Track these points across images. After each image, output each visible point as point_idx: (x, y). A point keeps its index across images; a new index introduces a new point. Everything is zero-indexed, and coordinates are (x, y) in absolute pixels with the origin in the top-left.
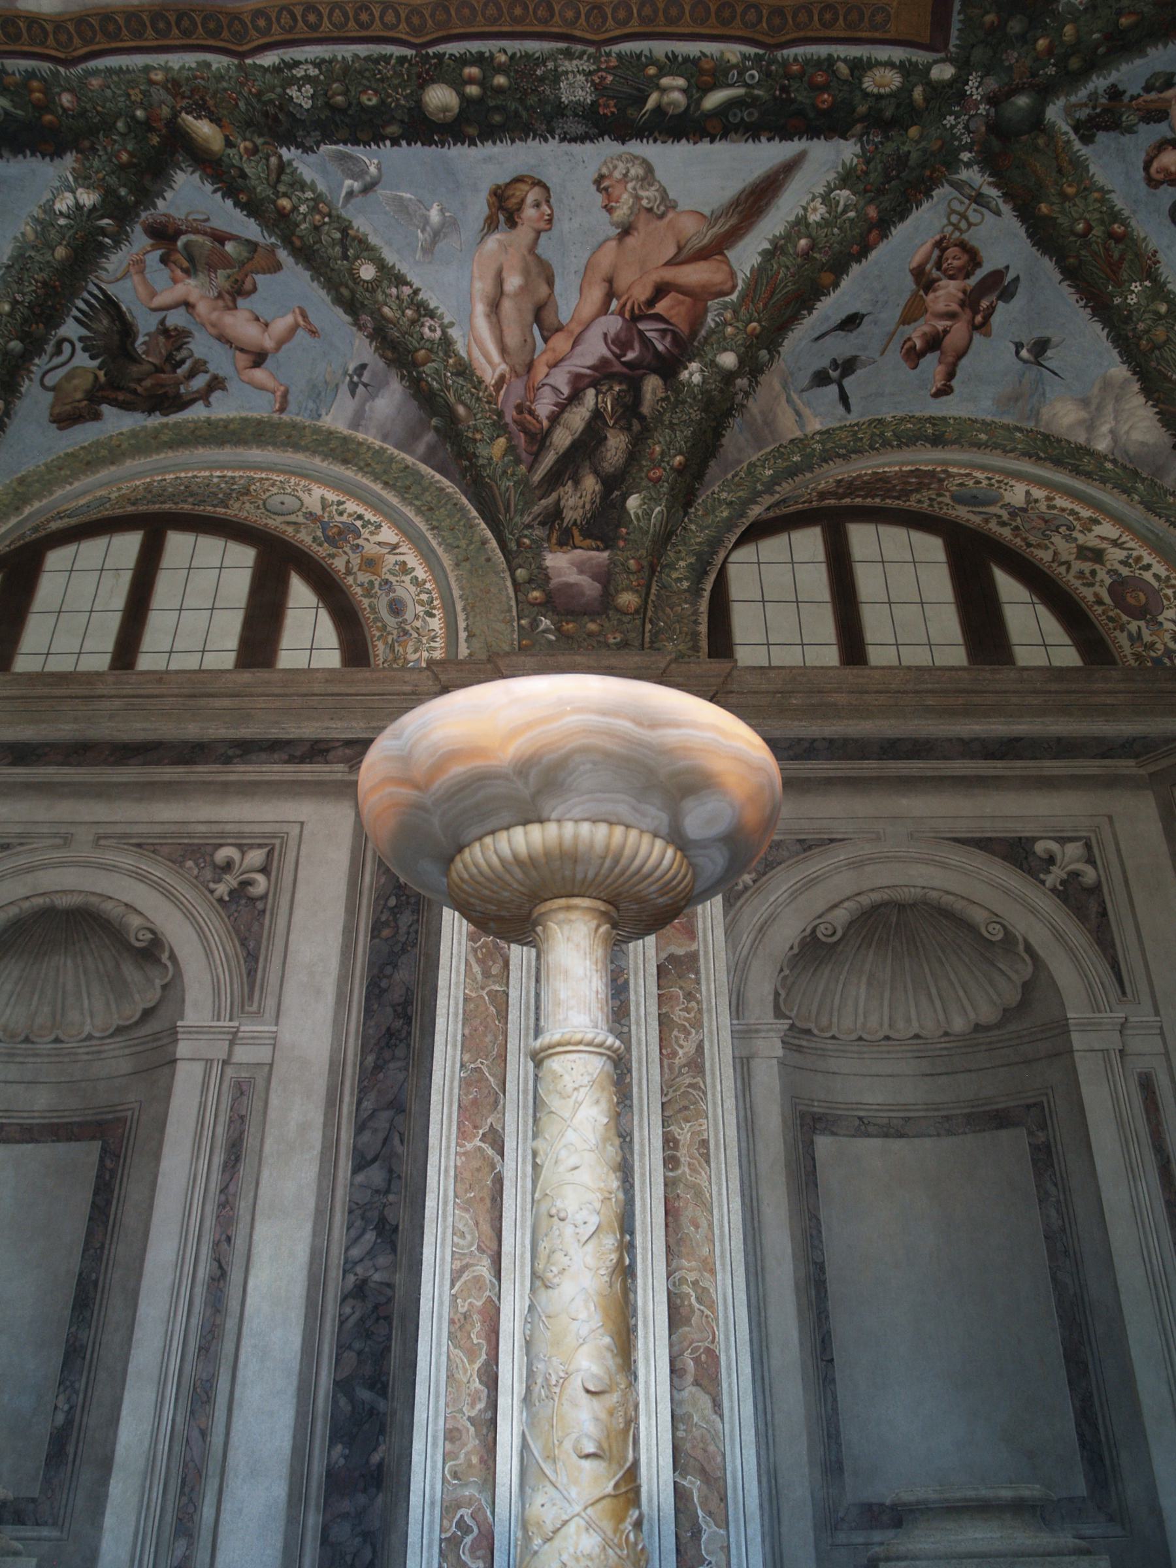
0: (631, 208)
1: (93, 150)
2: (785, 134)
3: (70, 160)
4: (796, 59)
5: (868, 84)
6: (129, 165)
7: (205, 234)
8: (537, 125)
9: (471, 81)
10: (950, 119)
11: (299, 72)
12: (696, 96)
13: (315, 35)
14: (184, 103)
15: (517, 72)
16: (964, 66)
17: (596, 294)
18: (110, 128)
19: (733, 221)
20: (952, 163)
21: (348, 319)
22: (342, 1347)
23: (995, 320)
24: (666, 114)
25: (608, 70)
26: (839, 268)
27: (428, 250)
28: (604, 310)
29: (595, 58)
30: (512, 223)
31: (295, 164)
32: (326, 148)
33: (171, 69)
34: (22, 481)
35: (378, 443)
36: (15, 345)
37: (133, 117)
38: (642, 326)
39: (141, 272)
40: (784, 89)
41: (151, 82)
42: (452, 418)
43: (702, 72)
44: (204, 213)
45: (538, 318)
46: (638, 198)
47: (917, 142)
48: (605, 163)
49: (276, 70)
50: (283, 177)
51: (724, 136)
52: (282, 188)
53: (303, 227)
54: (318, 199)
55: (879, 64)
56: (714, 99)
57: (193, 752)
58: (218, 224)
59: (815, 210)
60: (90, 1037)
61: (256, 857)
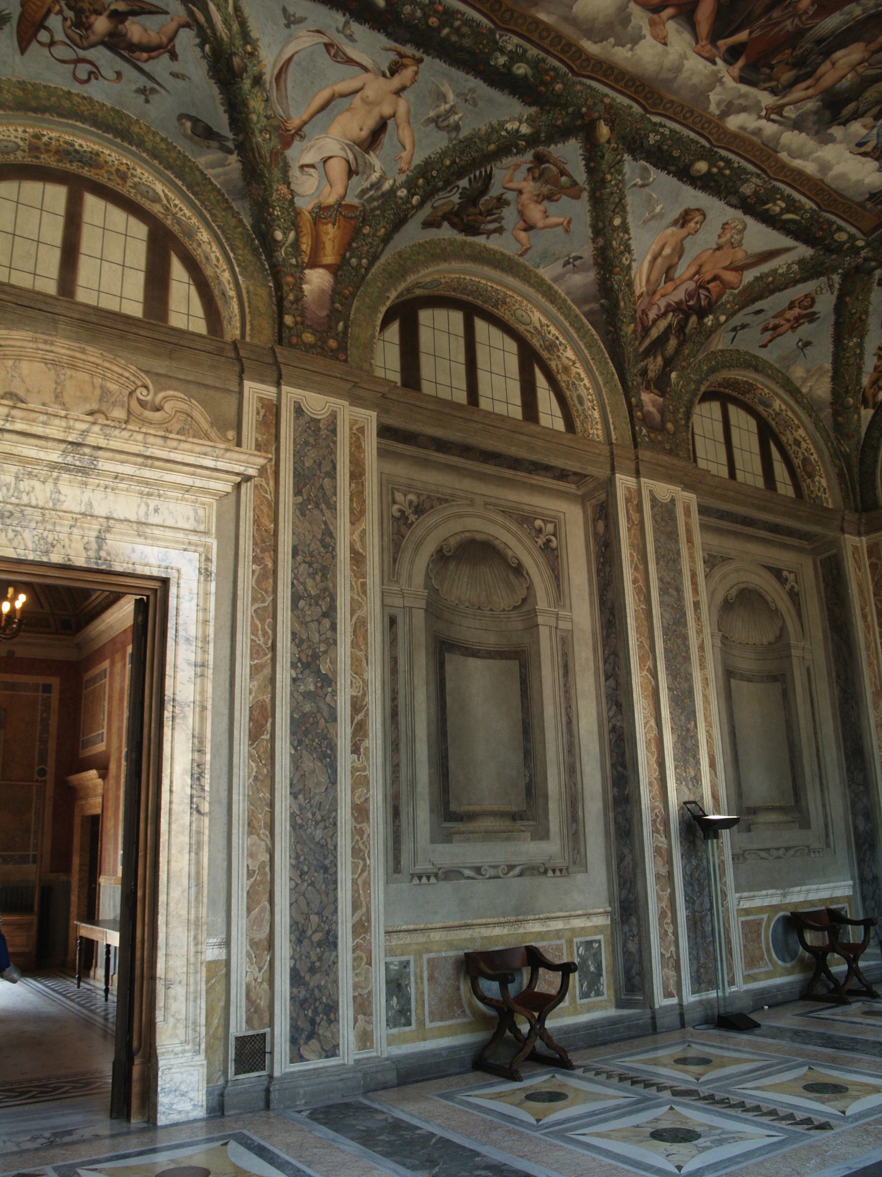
1: (549, 112)
2: (797, 238)
3: (533, 110)
5: (836, 236)
7: (558, 168)
11: (661, 130)
14: (607, 116)
16: (868, 245)
17: (693, 270)
18: (565, 107)
20: (834, 270)
21: (591, 236)
22: (611, 751)
23: (801, 328)
26: (772, 292)
27: (645, 222)
28: (691, 279)
29: (765, 182)
30: (683, 226)
34: (400, 255)
35: (563, 295)
36: (440, 184)
37: (580, 110)
38: (701, 291)
39: (515, 170)
41: (602, 101)
42: (616, 305)
45: (667, 272)
49: (655, 124)
57: (515, 463)
58: (569, 168)
60: (504, 610)
61: (550, 528)
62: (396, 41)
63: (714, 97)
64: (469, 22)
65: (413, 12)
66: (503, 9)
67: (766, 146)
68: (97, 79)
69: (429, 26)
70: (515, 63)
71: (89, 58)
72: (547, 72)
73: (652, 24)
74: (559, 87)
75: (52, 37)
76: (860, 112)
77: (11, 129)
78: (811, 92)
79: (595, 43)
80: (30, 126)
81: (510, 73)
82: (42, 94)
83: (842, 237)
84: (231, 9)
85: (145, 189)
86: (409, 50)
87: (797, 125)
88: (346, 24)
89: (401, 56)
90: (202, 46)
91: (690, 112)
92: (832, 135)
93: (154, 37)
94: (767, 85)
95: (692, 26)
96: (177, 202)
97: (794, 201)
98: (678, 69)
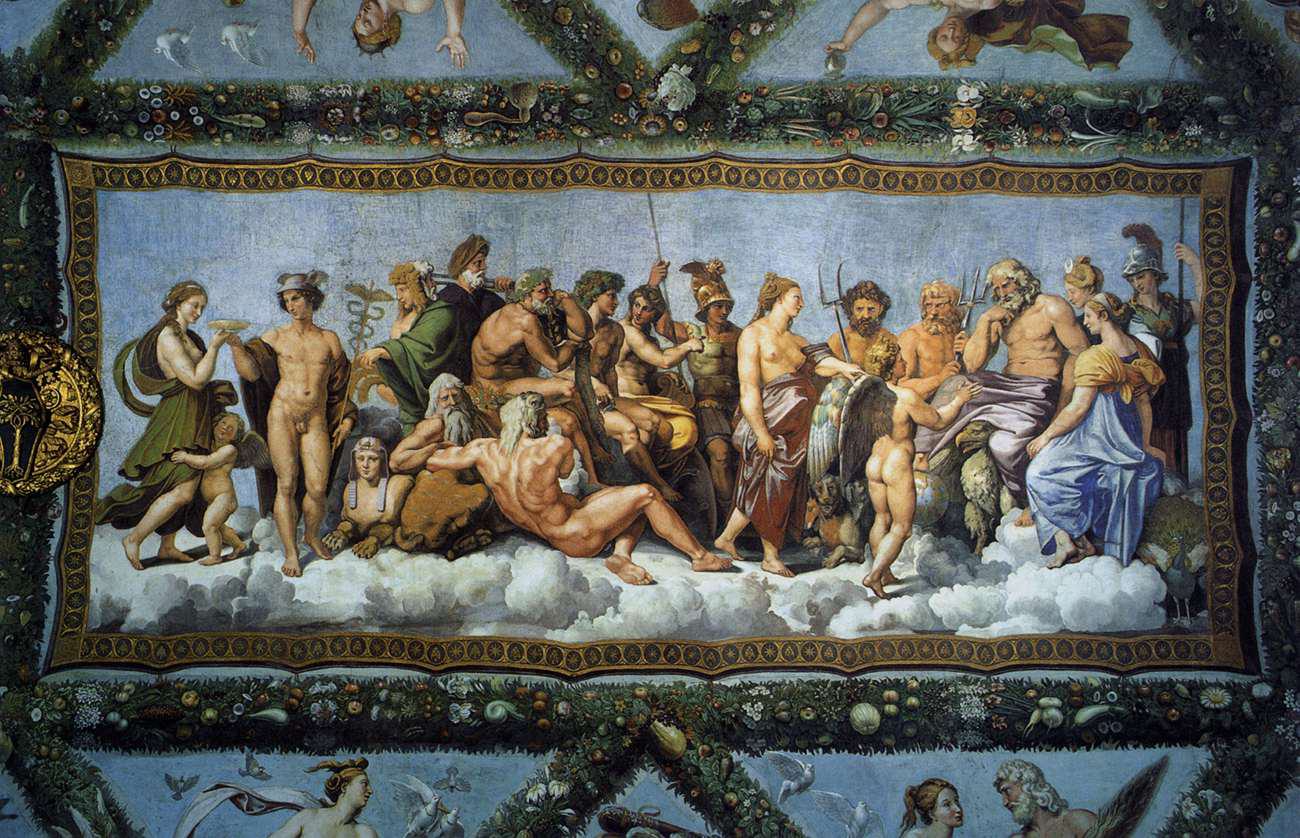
0: (1028, 807)
1: (574, 747)
2: (1149, 742)
3: (551, 756)
4: (1144, 683)
6: (602, 762)
8: (942, 737)
9: (890, 702)
10: (1280, 729)
11: (754, 692)
12: (1070, 713)
13: (770, 664)
15: (926, 694)
16: (1278, 685)
18: (591, 729)
19: (1119, 818)
24: (1047, 727)
25: (997, 693)
29: (988, 685)
30: (928, 821)
31: (742, 766)
32: (769, 753)
33: (653, 686)
37: (614, 723)
40: (1139, 706)
41: (635, 696)
43: (1072, 693)
44: (656, 808)
46: (1033, 798)
47: (1259, 747)
48: (1002, 768)
49: (737, 689)
50: (732, 775)
51: (1097, 745)
52: (731, 785)
53: (746, 819)
54: (760, 795)
55: (1210, 685)
56: (1085, 715)
58: (667, 818)
59: (1188, 808)
62: (321, 753)
63: (780, 608)
64: (396, 686)
65: (325, 708)
66: (426, 648)
67: (923, 632)
69: (352, 716)
70: (484, 707)
72: (532, 696)
73: (615, 569)
74: (562, 708)
76: (990, 512)
78: (896, 529)
79: (565, 628)
81: (487, 723)
83: (1217, 699)
84: (101, 808)
86: (342, 757)
87: (932, 580)
88: (249, 760)
89: (336, 769)
91: (765, 647)
92: (994, 563)
94: (836, 555)
95: (664, 543)
97: (1066, 685)
98: (697, 602)
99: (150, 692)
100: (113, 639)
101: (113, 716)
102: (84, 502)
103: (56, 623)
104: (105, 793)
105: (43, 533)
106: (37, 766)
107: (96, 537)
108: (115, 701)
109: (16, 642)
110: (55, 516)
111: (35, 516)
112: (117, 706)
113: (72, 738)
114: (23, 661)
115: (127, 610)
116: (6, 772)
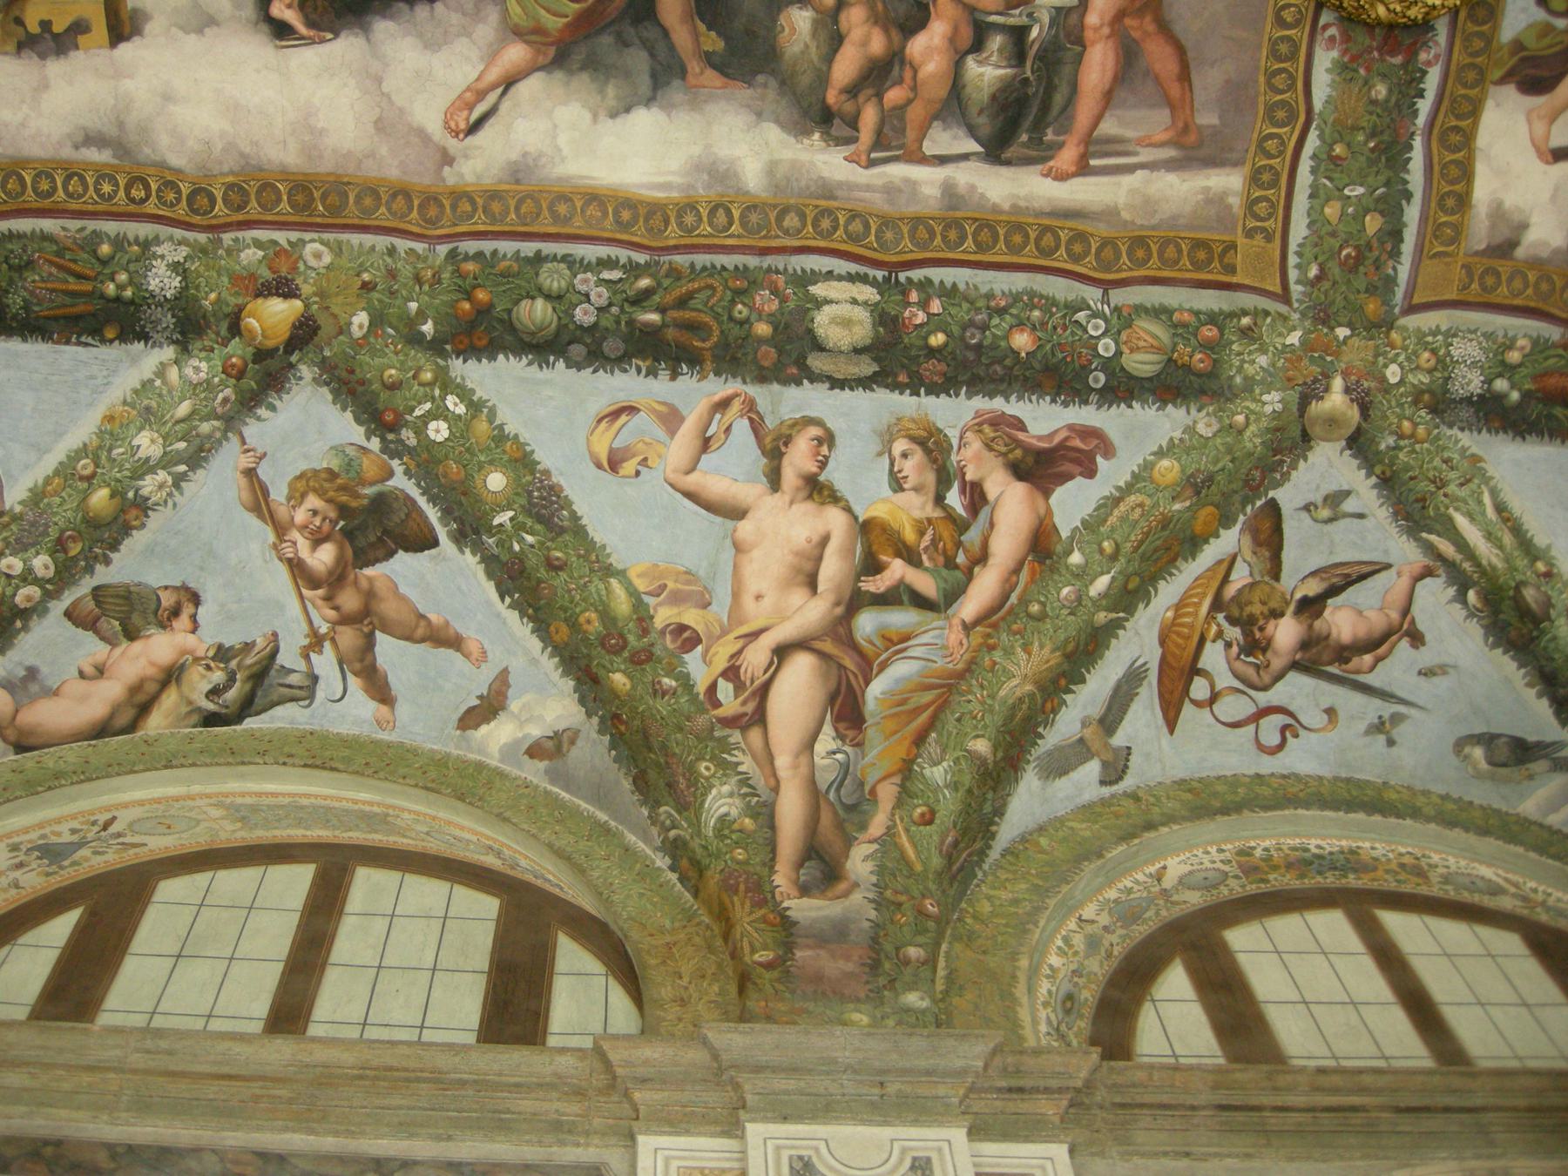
68: (1296, 736)
71: (1275, 703)
75: (1212, 686)
77: (1200, 852)
80: (1226, 841)
82: (1220, 788)
84: (1490, 512)
85: (1466, 881)
90: (1461, 598)
93: (1376, 621)
96: (1532, 884)
99: (1552, 352)
100: (1504, 268)
101: (1501, 385)
102: (1478, 44)
103: (1421, 235)
104: (1494, 493)
105: (1410, 87)
106: (1397, 448)
107: (1490, 104)
108: (1503, 363)
109: (1359, 259)
110: (1429, 64)
111: (1398, 60)
112: (1507, 370)
113: (1444, 411)
114: (1371, 290)
115: (1524, 226)
116: (1348, 452)
